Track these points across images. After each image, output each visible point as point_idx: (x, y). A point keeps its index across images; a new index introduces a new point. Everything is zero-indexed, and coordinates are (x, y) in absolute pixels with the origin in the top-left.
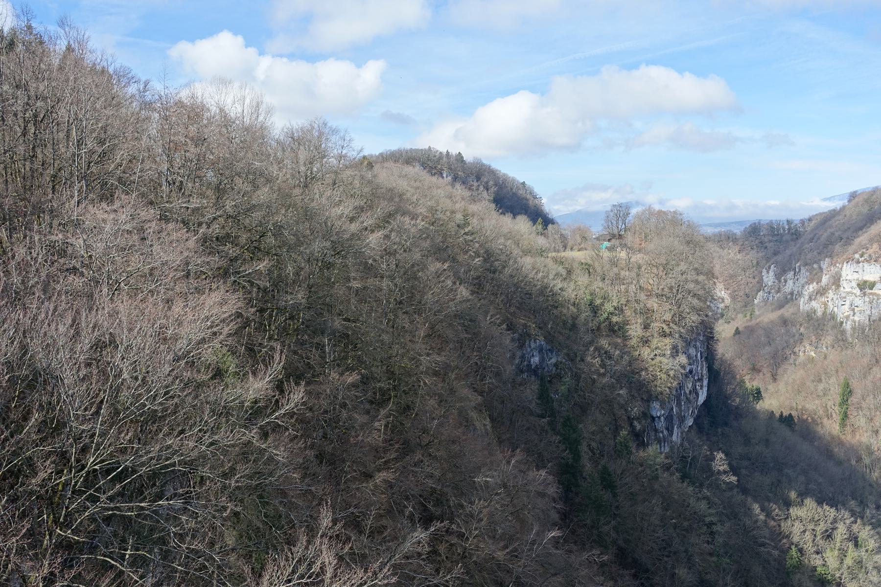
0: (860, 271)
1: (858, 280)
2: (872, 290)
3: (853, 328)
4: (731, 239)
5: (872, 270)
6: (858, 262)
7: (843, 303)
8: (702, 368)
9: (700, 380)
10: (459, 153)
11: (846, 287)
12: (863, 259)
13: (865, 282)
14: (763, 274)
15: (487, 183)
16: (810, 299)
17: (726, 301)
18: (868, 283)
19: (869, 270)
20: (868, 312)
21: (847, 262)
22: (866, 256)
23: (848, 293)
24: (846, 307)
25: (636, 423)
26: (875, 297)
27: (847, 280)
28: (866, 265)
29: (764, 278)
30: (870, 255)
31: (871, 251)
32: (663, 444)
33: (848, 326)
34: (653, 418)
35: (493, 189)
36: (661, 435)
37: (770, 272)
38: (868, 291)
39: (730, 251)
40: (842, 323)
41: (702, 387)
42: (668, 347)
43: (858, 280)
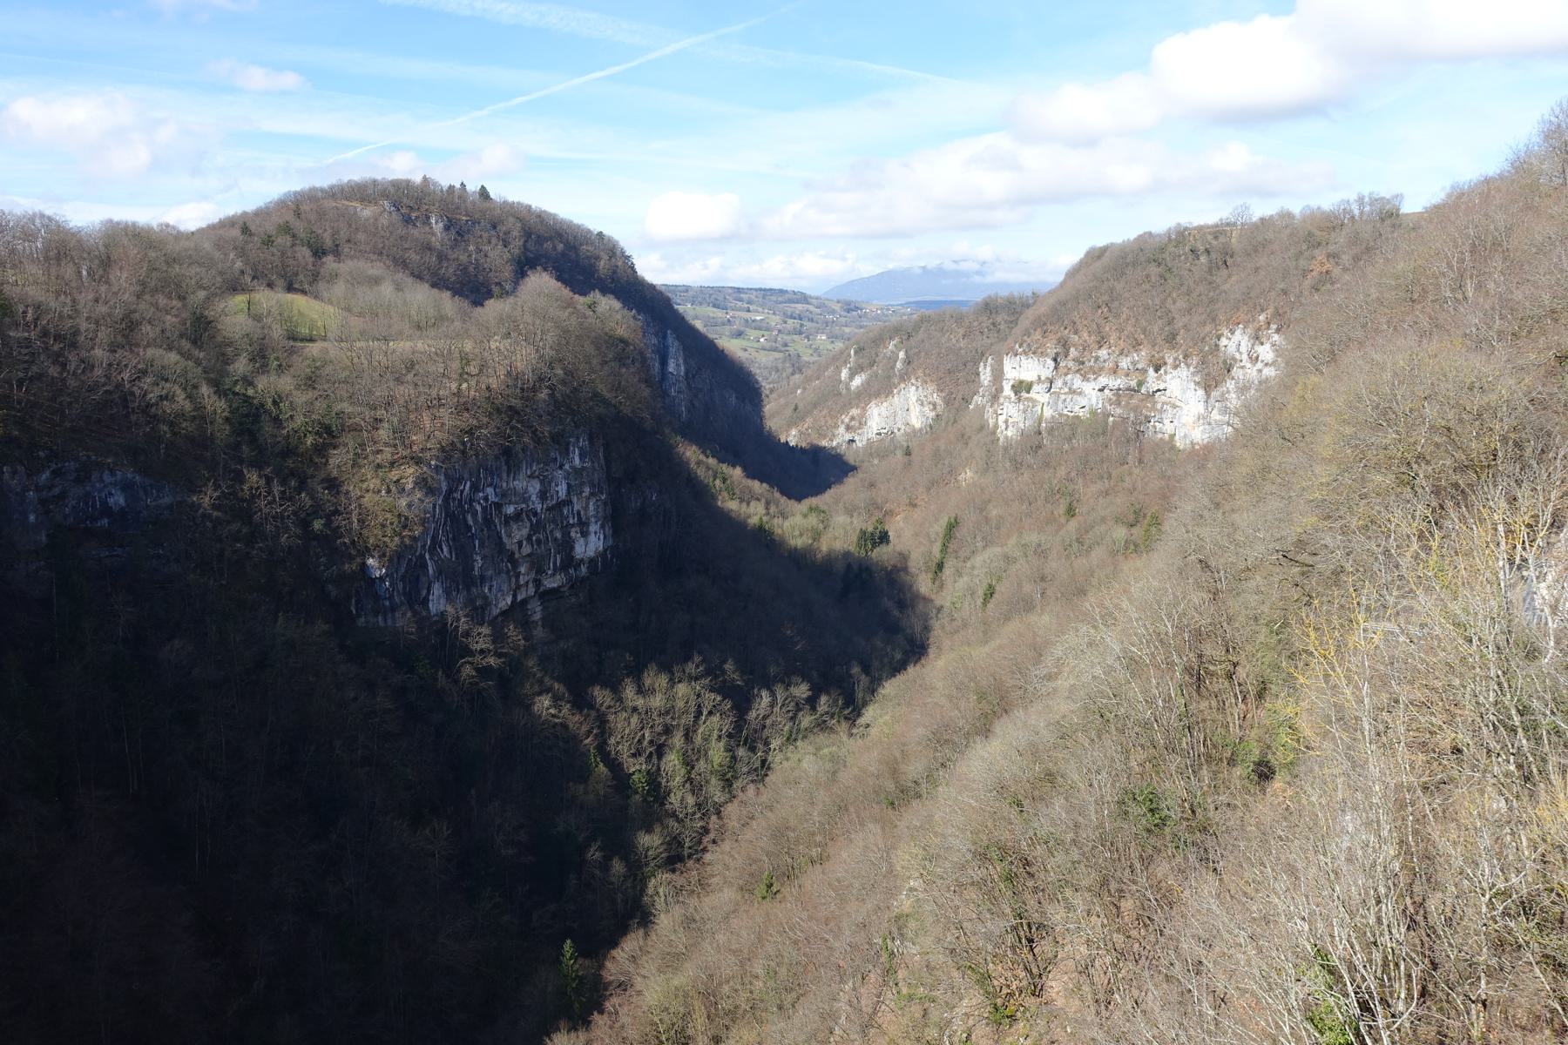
0: (1018, 367)
3: (1006, 449)
6: (1016, 355)
8: (586, 508)
9: (583, 526)
10: (482, 186)
11: (1007, 391)
13: (1021, 382)
15: (507, 233)
16: (991, 407)
22: (1025, 345)
23: (1006, 397)
25: (330, 587)
32: (390, 615)
34: (373, 581)
35: (517, 245)
36: (387, 603)
38: (1024, 395)
40: (998, 439)
41: (585, 534)
42: (410, 480)
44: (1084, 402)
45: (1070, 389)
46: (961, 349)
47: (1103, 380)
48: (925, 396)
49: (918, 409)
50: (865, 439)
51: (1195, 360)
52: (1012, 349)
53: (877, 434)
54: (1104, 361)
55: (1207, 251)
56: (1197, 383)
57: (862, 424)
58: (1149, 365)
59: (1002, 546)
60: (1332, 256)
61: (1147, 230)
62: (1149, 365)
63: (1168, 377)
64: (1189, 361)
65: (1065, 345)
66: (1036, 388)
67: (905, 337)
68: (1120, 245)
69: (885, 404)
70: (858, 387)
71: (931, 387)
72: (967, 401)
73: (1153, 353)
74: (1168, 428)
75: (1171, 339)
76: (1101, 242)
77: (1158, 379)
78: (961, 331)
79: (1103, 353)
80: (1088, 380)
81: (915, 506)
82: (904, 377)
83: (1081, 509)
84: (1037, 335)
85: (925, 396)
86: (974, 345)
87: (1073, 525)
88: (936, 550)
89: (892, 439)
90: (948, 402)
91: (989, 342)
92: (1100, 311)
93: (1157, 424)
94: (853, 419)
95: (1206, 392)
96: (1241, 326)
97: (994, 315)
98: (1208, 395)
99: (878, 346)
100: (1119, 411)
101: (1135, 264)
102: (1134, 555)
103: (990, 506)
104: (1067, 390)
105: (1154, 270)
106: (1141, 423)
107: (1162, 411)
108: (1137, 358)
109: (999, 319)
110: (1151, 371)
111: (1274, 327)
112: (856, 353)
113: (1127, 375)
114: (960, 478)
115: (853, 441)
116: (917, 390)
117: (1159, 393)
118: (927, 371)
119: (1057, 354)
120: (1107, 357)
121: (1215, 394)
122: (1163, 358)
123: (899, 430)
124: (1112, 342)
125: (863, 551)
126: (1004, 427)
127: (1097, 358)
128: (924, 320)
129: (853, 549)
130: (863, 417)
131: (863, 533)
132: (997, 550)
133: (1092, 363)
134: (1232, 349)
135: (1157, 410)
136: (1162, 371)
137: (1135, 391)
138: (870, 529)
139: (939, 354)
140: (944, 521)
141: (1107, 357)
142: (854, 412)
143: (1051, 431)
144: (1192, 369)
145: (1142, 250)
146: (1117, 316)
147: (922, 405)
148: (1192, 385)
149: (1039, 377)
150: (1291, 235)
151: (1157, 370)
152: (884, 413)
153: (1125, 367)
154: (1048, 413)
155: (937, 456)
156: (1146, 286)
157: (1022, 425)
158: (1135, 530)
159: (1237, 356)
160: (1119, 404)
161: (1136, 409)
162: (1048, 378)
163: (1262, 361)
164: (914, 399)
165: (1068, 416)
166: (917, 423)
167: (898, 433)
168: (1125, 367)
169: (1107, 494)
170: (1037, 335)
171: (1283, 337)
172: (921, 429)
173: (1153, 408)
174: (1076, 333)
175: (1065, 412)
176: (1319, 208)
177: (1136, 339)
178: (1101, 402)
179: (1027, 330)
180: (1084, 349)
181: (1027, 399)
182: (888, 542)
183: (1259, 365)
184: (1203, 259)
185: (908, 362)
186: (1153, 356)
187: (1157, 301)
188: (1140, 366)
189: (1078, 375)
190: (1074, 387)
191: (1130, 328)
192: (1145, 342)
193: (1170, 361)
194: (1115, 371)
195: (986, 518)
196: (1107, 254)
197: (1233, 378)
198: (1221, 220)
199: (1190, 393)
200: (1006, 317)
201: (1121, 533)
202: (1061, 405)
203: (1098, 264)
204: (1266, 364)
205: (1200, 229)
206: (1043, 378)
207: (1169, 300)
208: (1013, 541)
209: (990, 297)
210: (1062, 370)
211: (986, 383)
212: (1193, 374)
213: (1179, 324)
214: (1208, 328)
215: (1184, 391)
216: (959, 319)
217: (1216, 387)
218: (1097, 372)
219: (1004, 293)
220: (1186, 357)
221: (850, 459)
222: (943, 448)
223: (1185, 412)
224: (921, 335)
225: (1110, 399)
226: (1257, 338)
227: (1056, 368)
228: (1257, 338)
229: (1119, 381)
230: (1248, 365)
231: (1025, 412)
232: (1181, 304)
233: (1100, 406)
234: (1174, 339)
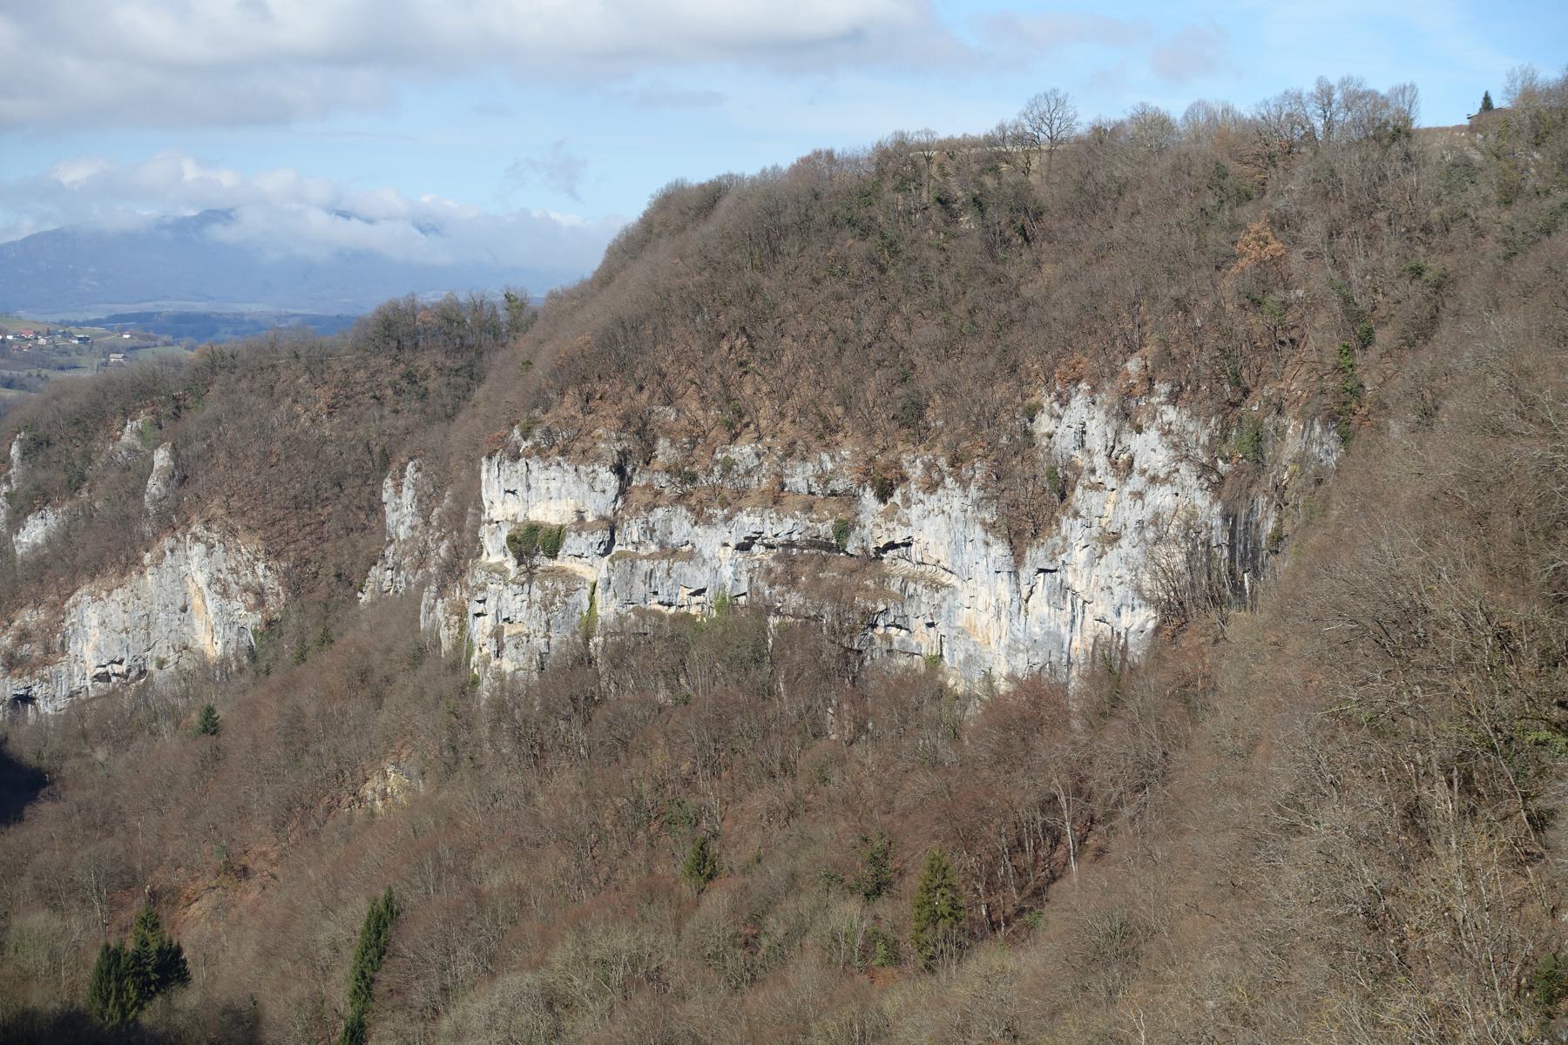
0: (521, 489)
1: (514, 522)
2: (555, 557)
3: (500, 707)
4: (303, 360)
5: (553, 485)
6: (515, 457)
7: (479, 608)
11: (494, 551)
12: (529, 443)
13: (533, 529)
14: (385, 497)
17: (271, 599)
18: (540, 535)
19: (543, 485)
20: (539, 642)
21: (490, 458)
22: (537, 432)
24: (487, 622)
26: (561, 586)
27: (491, 522)
28: (534, 466)
29: (387, 509)
30: (548, 432)
31: (548, 420)
33: (485, 690)
37: (405, 489)
39: (299, 409)
40: (476, 682)
43: (514, 522)
44: (702, 578)
45: (662, 545)
46: (324, 441)
47: (748, 522)
48: (234, 571)
49: (212, 606)
50: (62, 692)
51: (980, 470)
52: (503, 442)
53: (98, 677)
54: (748, 473)
55: (978, 204)
56: (990, 528)
57: (53, 647)
58: (861, 484)
59: (534, 967)
60: (1281, 223)
61: (824, 146)
62: (861, 484)
63: (915, 512)
64: (966, 472)
65: (644, 433)
66: (572, 543)
67: (169, 410)
68: (753, 179)
69: (118, 595)
70: (35, 547)
71: (249, 545)
72: (349, 581)
73: (872, 452)
74: (923, 641)
75: (912, 420)
76: (699, 172)
77: (889, 516)
78: (324, 396)
79: (743, 451)
80: (709, 521)
81: (245, 872)
82: (171, 520)
83: (732, 858)
84: (569, 405)
85: (234, 571)
86: (361, 432)
87: (718, 900)
88: (340, 994)
89: (141, 691)
90: (296, 586)
91: (401, 423)
92: (725, 346)
93: (893, 631)
94: (24, 636)
95: (1013, 548)
96: (1084, 386)
97: (408, 354)
98: (1018, 558)
99: (88, 436)
100: (794, 599)
101: (804, 226)
102: (889, 971)
103: (481, 862)
104: (653, 548)
105: (854, 247)
106: (853, 630)
107: (904, 598)
108: (830, 466)
109: (423, 363)
110: (869, 498)
111: (1163, 388)
112: (25, 453)
113: (809, 508)
114: (367, 791)
115: (27, 699)
116: (209, 554)
117: (891, 553)
118: (235, 503)
119: (624, 455)
120: (752, 462)
121: (1036, 556)
122: (897, 463)
123: (161, 664)
124: (763, 423)
125: (113, 1010)
126: (489, 649)
127: (728, 466)
128: (215, 365)
129: (82, 1002)
130: (53, 632)
131: (112, 956)
132: (517, 982)
133: (715, 478)
134: (1065, 441)
135: (890, 595)
136: (897, 498)
137: (828, 547)
138: (131, 946)
139: (267, 455)
140: (357, 911)
141: (752, 462)
142: (29, 617)
143: (618, 656)
144: (973, 491)
145: (817, 196)
146: (774, 358)
147: (225, 593)
148: (978, 533)
149: (580, 515)
150: (1176, 169)
151: (884, 494)
152: (118, 618)
153: (802, 486)
154: (607, 608)
155: (296, 734)
156: (831, 286)
157: (539, 642)
158: (883, 907)
159: (1080, 458)
160: (792, 582)
161: (835, 595)
162: (602, 518)
163: (1143, 472)
164: (201, 579)
165: (660, 616)
166: (211, 642)
167: (158, 675)
168: (802, 486)
169: (792, 814)
170: (569, 405)
171: (1186, 412)
172: (224, 661)
173: (882, 592)
174: (669, 403)
175: (653, 604)
176: (1226, 110)
177: (824, 419)
178: (744, 578)
179: (540, 391)
180: (693, 443)
181: (551, 572)
182: (183, 978)
183: (1136, 482)
184: (967, 222)
185: (181, 477)
186: (872, 460)
187: (868, 323)
188: (839, 485)
189: (682, 510)
190: (675, 539)
191: (806, 391)
192: (848, 423)
193: (916, 471)
194: (776, 497)
195: (477, 894)
196: (726, 202)
197: (1076, 514)
198: (1002, 128)
199: (972, 553)
200: (440, 359)
201: (848, 914)
202: (640, 589)
203: (710, 228)
204: (1153, 480)
205: (951, 149)
206: (590, 518)
207: (896, 322)
208: (562, 954)
209: (395, 308)
210: (638, 498)
211: (403, 532)
212: (978, 504)
213: (927, 381)
214: (1001, 391)
215: (957, 547)
216: (316, 362)
217: (1035, 535)
218: (733, 501)
219: (431, 296)
220: (955, 462)
221: (24, 749)
222: (311, 710)
223: (964, 598)
224: (213, 405)
225: (769, 571)
226: (1126, 417)
227: (623, 491)
228: (1126, 417)
229: (789, 524)
230: (1111, 482)
231: (546, 606)
232: (929, 331)
233: (744, 588)
234: (921, 416)
